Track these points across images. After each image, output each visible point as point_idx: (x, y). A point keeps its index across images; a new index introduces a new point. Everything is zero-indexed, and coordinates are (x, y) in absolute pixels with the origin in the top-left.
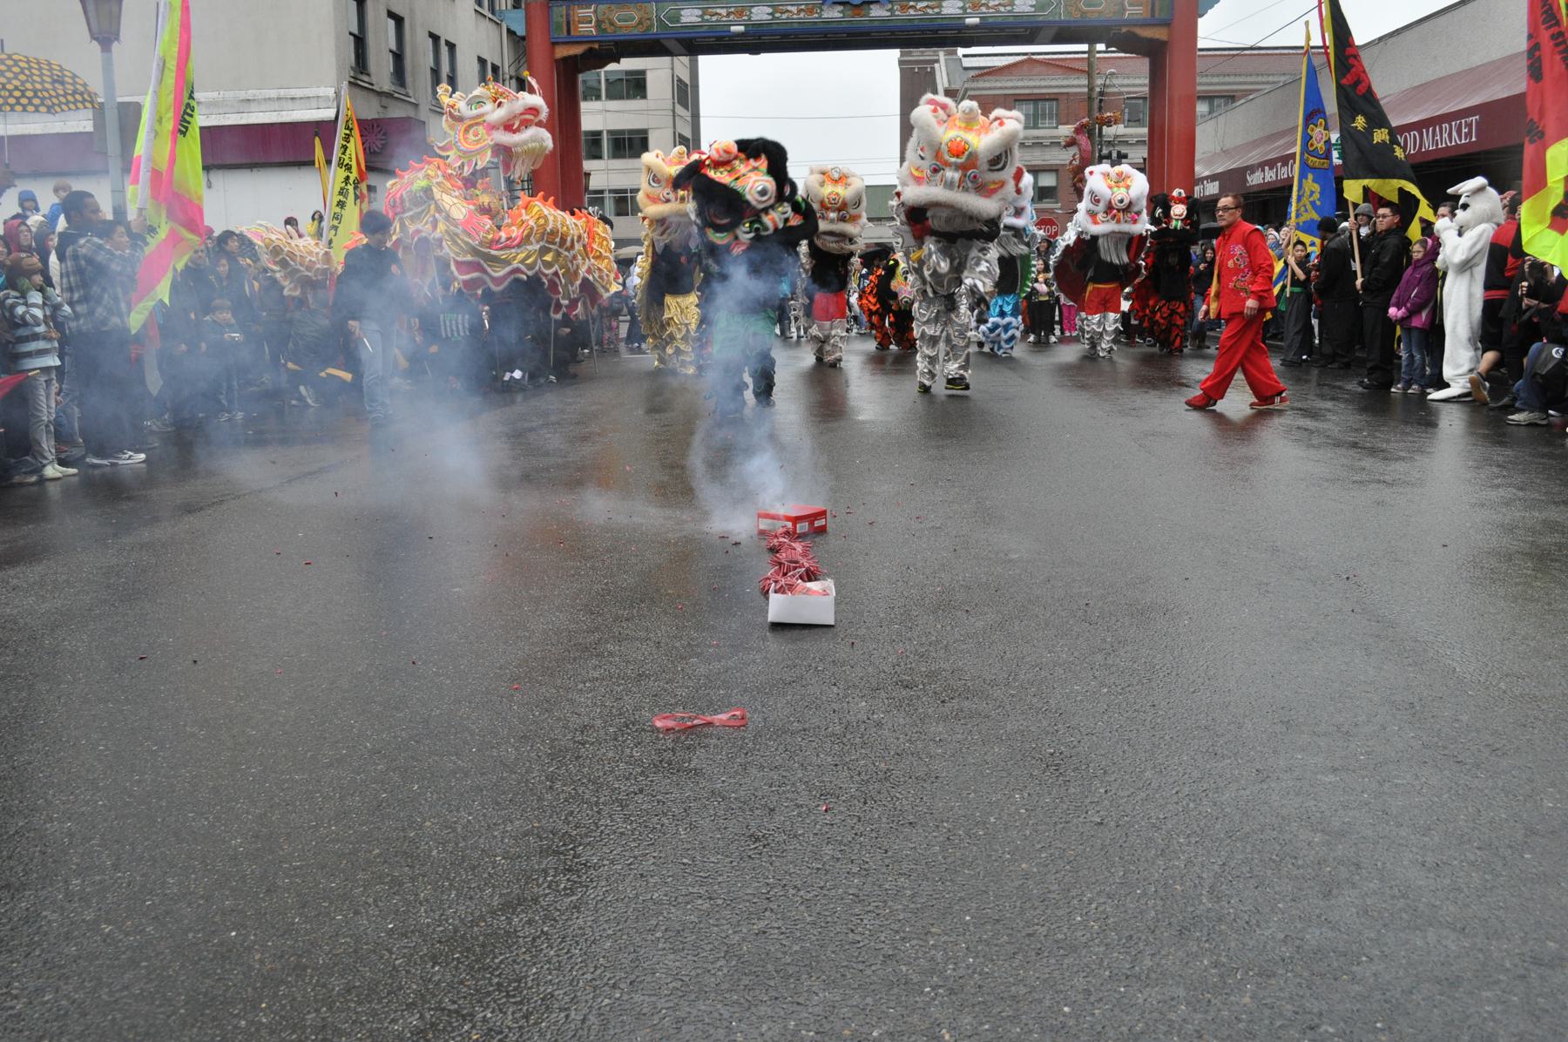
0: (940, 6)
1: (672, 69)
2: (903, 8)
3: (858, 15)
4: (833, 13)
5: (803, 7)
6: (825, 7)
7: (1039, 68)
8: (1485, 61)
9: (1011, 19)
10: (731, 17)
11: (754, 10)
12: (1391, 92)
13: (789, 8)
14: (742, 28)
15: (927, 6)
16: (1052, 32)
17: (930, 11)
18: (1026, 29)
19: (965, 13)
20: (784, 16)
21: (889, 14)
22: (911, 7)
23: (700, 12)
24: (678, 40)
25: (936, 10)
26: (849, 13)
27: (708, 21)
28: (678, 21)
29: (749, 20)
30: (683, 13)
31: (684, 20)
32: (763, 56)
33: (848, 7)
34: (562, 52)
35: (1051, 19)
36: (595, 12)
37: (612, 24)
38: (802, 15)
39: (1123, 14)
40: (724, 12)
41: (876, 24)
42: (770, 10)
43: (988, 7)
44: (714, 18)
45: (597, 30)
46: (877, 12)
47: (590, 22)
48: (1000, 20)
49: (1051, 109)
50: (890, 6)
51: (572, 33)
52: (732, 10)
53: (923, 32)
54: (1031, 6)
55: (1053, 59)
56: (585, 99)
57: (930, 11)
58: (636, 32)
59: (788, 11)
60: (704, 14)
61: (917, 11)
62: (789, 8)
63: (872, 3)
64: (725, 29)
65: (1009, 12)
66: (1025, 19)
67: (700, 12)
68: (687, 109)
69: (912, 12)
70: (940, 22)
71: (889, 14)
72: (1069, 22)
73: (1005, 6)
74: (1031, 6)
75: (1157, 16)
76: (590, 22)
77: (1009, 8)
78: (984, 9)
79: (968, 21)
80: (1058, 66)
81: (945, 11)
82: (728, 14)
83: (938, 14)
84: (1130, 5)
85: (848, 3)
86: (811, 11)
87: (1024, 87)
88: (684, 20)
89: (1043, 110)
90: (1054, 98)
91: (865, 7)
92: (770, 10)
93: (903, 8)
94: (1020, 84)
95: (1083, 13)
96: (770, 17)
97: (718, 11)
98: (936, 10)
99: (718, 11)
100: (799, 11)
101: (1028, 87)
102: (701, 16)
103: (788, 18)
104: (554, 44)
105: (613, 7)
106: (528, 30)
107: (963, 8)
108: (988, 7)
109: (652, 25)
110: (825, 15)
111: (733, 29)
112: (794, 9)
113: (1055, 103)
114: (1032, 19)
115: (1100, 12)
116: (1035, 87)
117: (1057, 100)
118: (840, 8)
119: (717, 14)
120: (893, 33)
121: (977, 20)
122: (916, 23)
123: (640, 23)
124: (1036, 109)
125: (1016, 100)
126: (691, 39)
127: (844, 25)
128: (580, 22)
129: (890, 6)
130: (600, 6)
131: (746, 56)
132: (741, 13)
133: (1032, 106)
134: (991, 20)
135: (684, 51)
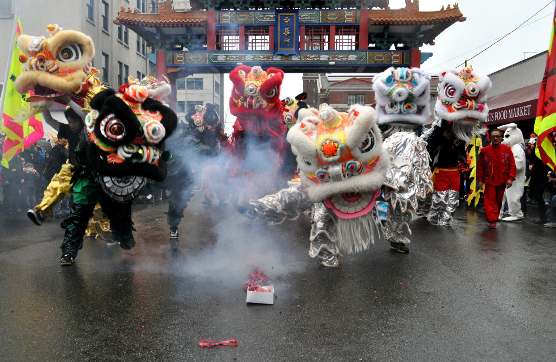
0: (319, 57)
1: (213, 78)
2: (305, 57)
3: (287, 59)
4: (278, 59)
5: (266, 56)
6: (274, 56)
7: (357, 82)
8: (533, 84)
9: (347, 63)
10: (237, 59)
11: (246, 57)
12: (497, 95)
13: (260, 56)
15: (314, 57)
16: (363, 68)
17: (315, 59)
18: (353, 67)
19: (329, 60)
20: (258, 59)
21: (299, 60)
22: (308, 57)
23: (225, 57)
25: (318, 59)
26: (284, 59)
28: (216, 60)
29: (244, 60)
30: (218, 57)
31: (219, 59)
33: (284, 56)
34: (170, 70)
35: (363, 63)
36: (184, 55)
37: (190, 60)
38: (265, 59)
39: (391, 62)
40: (234, 57)
41: (294, 63)
42: (253, 57)
43: (338, 58)
44: (231, 59)
45: (184, 63)
46: (295, 59)
47: (182, 59)
48: (343, 63)
49: (362, 98)
50: (300, 57)
51: (175, 63)
52: (238, 56)
53: (313, 67)
54: (355, 58)
55: (365, 79)
56: (179, 89)
57: (315, 59)
58: (200, 63)
59: (260, 57)
60: (227, 56)
61: (311, 58)
62: (260, 56)
63: (292, 55)
64: (235, 63)
65: (346, 60)
66: (353, 63)
67: (225, 57)
68: (218, 93)
69: (308, 59)
70: (319, 63)
71: (299, 60)
72: (370, 64)
73: (345, 58)
74: (355, 58)
75: (404, 63)
76: (182, 59)
77: (346, 59)
78: (336, 59)
79: (330, 63)
80: (365, 81)
81: (321, 59)
82: (236, 58)
83: (318, 60)
84: (394, 59)
85: (283, 55)
86: (268, 58)
87: (351, 89)
88: (219, 59)
89: (359, 98)
90: (364, 93)
91: (290, 56)
92: (253, 57)
93: (305, 57)
94: (350, 88)
95: (376, 61)
96: (253, 60)
97: (232, 56)
98: (318, 59)
99: (232, 56)
100: (264, 58)
101: (353, 89)
102: (226, 58)
103: (260, 60)
104: (167, 67)
105: (191, 54)
106: (157, 62)
107: (328, 58)
108: (338, 58)
109: (206, 61)
110: (274, 59)
112: (262, 57)
113: (364, 96)
114: (355, 63)
115: (382, 61)
116: (356, 89)
117: (364, 94)
118: (280, 57)
120: (301, 67)
121: (333, 63)
122: (310, 63)
123: (201, 60)
124: (356, 98)
125: (348, 94)
126: (221, 67)
127: (282, 63)
128: (178, 59)
129: (300, 57)
130: (186, 53)
132: (241, 58)
133: (355, 97)
134: (339, 63)
135: (218, 71)
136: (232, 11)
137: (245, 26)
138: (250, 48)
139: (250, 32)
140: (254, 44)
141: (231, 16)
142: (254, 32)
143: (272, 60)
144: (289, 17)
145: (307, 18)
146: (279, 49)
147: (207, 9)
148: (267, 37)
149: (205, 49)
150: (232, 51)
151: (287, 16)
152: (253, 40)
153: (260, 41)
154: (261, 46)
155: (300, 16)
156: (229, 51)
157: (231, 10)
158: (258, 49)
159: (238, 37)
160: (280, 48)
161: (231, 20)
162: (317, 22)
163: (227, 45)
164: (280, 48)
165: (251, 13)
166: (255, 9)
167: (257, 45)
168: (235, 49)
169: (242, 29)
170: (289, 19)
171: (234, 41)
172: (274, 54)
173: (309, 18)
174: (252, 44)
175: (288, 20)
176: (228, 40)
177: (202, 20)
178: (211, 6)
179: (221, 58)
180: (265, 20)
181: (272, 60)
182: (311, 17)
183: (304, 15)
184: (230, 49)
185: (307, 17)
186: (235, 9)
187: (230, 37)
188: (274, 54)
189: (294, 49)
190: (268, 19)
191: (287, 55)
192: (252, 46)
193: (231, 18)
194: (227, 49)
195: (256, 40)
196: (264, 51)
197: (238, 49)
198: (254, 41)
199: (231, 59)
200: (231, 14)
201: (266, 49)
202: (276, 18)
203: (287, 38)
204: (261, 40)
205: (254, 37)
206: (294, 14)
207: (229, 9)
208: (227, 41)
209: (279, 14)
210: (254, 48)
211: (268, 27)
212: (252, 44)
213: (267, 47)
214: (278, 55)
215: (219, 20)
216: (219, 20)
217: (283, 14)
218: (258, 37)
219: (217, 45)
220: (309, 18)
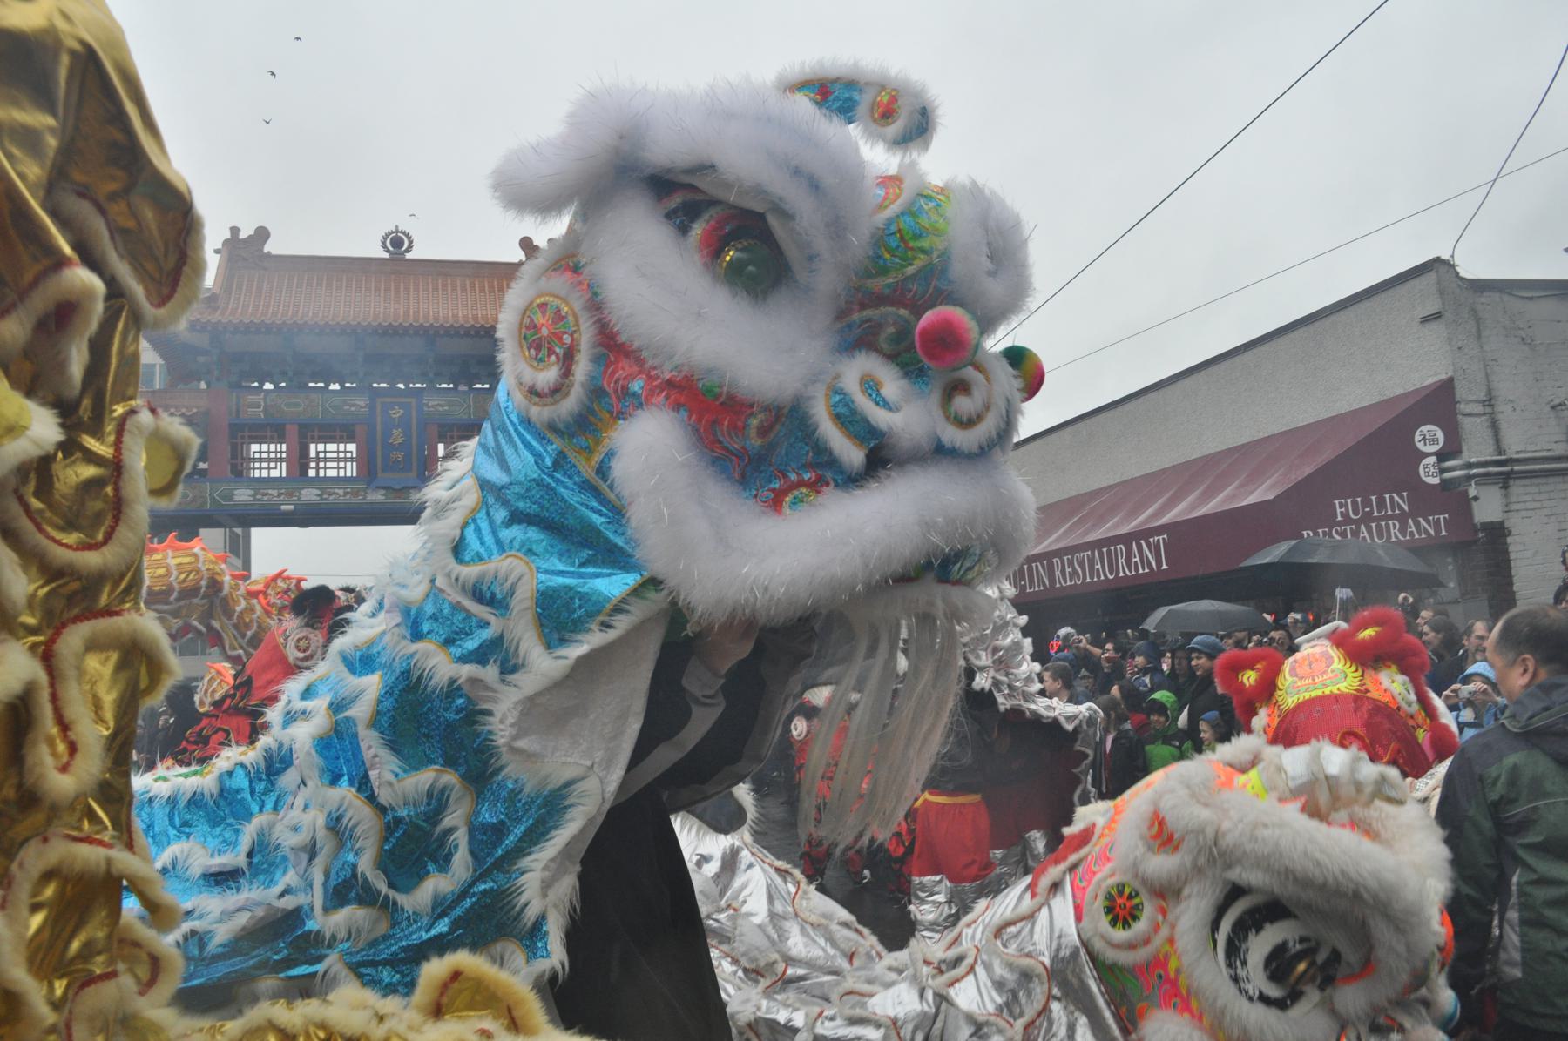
4: (377, 496)
6: (369, 491)
10: (282, 498)
11: (303, 492)
13: (336, 491)
14: (292, 507)
20: (331, 498)
23: (252, 492)
24: (231, 515)
27: (259, 500)
28: (231, 500)
29: (299, 499)
30: (236, 492)
31: (237, 498)
32: (311, 529)
38: (348, 497)
40: (275, 493)
42: (318, 492)
44: (265, 498)
60: (257, 491)
62: (336, 491)
67: (252, 492)
68: (238, 557)
82: (280, 495)
86: (357, 494)
88: (237, 498)
92: (318, 492)
97: (270, 491)
99: (270, 491)
100: (346, 494)
102: (254, 496)
111: (283, 507)
112: (341, 492)
118: (383, 492)
119: (268, 494)
123: (194, 500)
131: (296, 529)
132: (292, 496)
136: (268, 391)
137: (299, 425)
138: (312, 473)
139: (313, 437)
140: (322, 465)
141: (265, 402)
142: (319, 437)
143: (364, 499)
144: (401, 405)
145: (440, 409)
146: (379, 475)
147: (208, 384)
148: (352, 447)
149: (203, 473)
150: (270, 480)
151: (399, 404)
152: (318, 453)
153: (335, 455)
154: (338, 468)
155: (427, 405)
156: (261, 480)
157: (268, 386)
158: (332, 473)
159: (284, 446)
160: (383, 471)
161: (265, 411)
162: (466, 417)
163: (257, 465)
164: (383, 471)
165: (314, 396)
166: (322, 385)
167: (328, 465)
168: (275, 474)
169: (293, 432)
170: (402, 411)
171: (273, 455)
172: (369, 485)
173: (446, 408)
174: (318, 464)
175: (397, 413)
176: (260, 452)
177: (195, 410)
178: (218, 379)
179: (243, 495)
180: (346, 411)
181: (364, 499)
182: (449, 406)
183: (436, 403)
184: (265, 474)
185: (442, 406)
186: (276, 386)
187: (265, 447)
188: (369, 485)
189: (413, 474)
190: (353, 409)
191: (398, 487)
192: (317, 468)
193: (265, 406)
194: (257, 475)
195: (325, 452)
196: (346, 479)
197: (284, 475)
198: (322, 455)
199: (265, 498)
200: (265, 398)
201: (349, 474)
202: (372, 407)
203: (396, 450)
204: (338, 452)
205: (321, 447)
206: (413, 400)
207: (262, 384)
208: (257, 455)
209: (379, 400)
210: (322, 473)
211: (353, 425)
212: (318, 464)
213: (351, 470)
214: (378, 488)
215: (238, 411)
216: (238, 411)
217: (388, 400)
218: (331, 447)
219: (232, 464)
220: (446, 408)
